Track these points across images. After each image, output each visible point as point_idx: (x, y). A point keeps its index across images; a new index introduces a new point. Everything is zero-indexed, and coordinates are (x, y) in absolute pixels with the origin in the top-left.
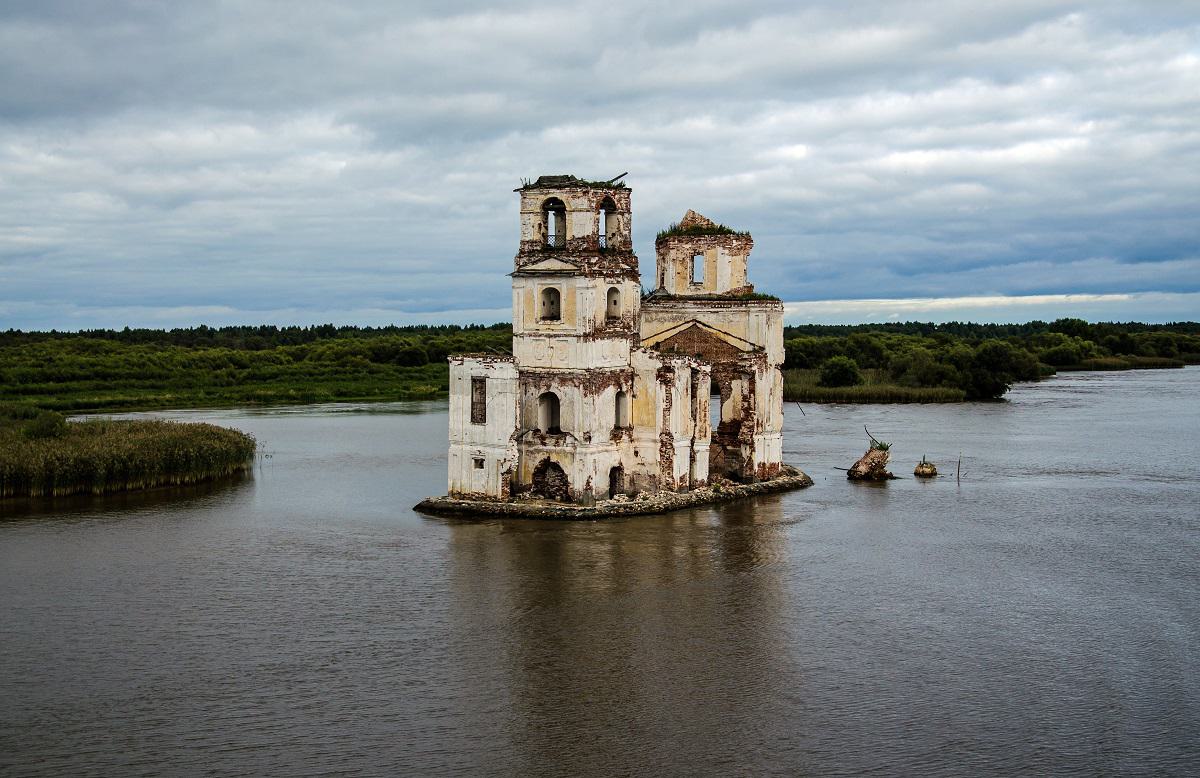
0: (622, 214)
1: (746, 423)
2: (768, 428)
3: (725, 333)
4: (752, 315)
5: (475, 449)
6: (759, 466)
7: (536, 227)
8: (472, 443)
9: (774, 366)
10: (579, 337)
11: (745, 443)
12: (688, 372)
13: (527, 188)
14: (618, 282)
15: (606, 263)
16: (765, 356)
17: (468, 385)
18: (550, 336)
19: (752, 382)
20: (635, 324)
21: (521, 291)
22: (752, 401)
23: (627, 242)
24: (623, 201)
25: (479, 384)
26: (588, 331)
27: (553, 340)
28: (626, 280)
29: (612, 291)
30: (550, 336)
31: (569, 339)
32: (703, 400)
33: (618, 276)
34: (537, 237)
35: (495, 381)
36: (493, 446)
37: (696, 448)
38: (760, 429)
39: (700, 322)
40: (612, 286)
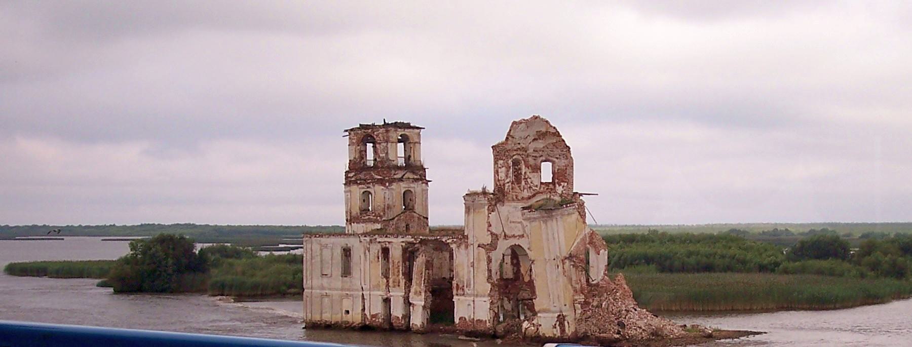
0: (380, 144)
9: (476, 245)
14: (368, 187)
20: (384, 214)
28: (376, 185)
29: (367, 194)
38: (460, 292)
40: (365, 190)
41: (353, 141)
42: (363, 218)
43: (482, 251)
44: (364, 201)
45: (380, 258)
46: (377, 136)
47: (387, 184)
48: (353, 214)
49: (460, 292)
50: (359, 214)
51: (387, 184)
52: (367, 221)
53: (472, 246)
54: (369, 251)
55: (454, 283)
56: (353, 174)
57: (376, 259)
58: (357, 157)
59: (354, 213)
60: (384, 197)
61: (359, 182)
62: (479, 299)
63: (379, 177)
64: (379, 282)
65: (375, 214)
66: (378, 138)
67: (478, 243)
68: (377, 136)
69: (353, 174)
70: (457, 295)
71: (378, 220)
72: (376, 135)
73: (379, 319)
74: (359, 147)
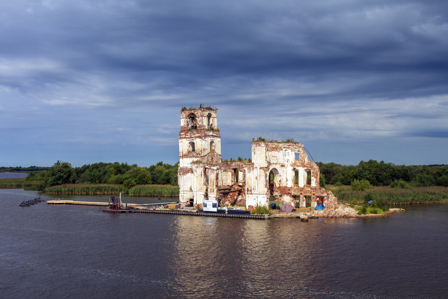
0: (198, 117)
2: (253, 192)
9: (258, 168)
14: (192, 140)
15: (189, 134)
28: (197, 139)
38: (249, 192)
40: (190, 141)
41: (183, 116)
42: (189, 155)
43: (262, 171)
45: (203, 175)
46: (197, 113)
47: (203, 138)
49: (249, 192)
50: (187, 153)
51: (203, 138)
52: (192, 157)
53: (256, 169)
54: (196, 172)
55: (246, 188)
56: (184, 133)
57: (200, 176)
58: (185, 124)
59: (184, 153)
60: (202, 145)
62: (260, 196)
64: (202, 187)
67: (260, 167)
68: (197, 113)
69: (184, 133)
70: (247, 194)
71: (198, 156)
72: (196, 113)
74: (187, 120)
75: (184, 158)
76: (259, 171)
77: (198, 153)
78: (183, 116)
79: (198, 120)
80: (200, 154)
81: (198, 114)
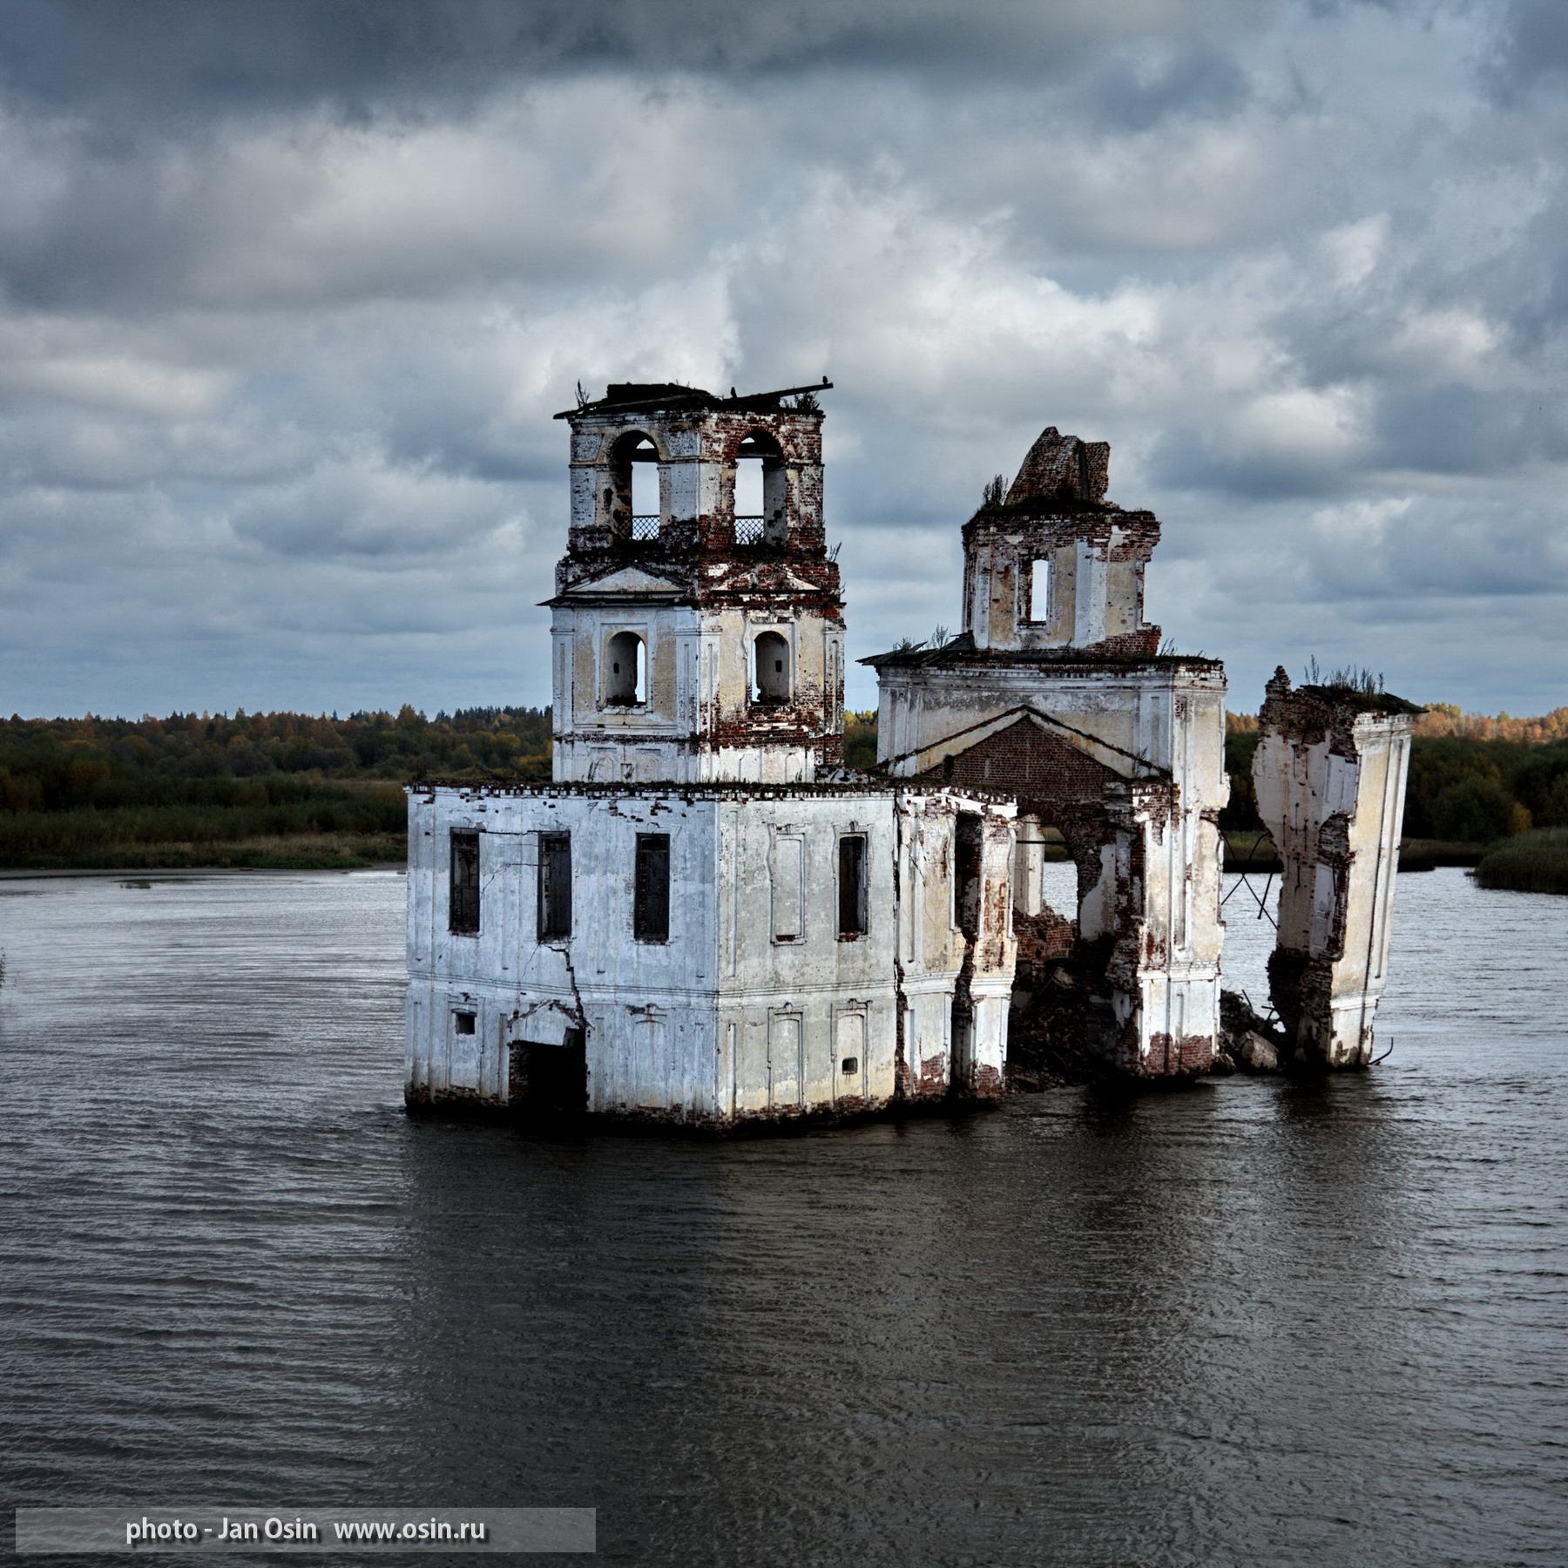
0: (799, 468)
1: (1123, 943)
2: (1176, 953)
3: (1090, 737)
4: (1147, 698)
5: (459, 988)
6: (1154, 1039)
7: (601, 497)
8: (453, 977)
10: (680, 741)
11: (1121, 989)
12: (951, 821)
13: (586, 410)
14: (782, 620)
16: (1173, 791)
17: (444, 846)
18: (623, 740)
19: (1138, 849)
20: (828, 713)
21: (567, 639)
22: (1136, 893)
23: (813, 531)
24: (800, 439)
25: (466, 846)
26: (700, 728)
27: (631, 749)
28: (804, 614)
29: (768, 643)
30: (623, 740)
31: (663, 746)
32: (996, 882)
33: (784, 606)
34: (601, 519)
35: (497, 840)
36: (494, 982)
37: (975, 990)
38: (1157, 958)
39: (1037, 713)
40: (766, 628)
41: (715, 446)
42: (755, 728)
44: (616, 668)
48: (723, 717)
50: (744, 714)
52: (769, 741)
56: (725, 567)
61: (746, 598)
63: (812, 587)
65: (799, 714)
66: (790, 448)
67: (1202, 807)
68: (790, 438)
69: (725, 567)
70: (1146, 969)
73: (941, 1075)
75: (726, 747)
76: (1197, 833)
77: (805, 713)
78: (715, 446)
79: (796, 484)
80: (813, 722)
81: (795, 447)
